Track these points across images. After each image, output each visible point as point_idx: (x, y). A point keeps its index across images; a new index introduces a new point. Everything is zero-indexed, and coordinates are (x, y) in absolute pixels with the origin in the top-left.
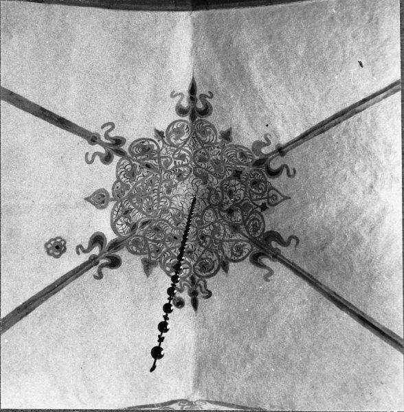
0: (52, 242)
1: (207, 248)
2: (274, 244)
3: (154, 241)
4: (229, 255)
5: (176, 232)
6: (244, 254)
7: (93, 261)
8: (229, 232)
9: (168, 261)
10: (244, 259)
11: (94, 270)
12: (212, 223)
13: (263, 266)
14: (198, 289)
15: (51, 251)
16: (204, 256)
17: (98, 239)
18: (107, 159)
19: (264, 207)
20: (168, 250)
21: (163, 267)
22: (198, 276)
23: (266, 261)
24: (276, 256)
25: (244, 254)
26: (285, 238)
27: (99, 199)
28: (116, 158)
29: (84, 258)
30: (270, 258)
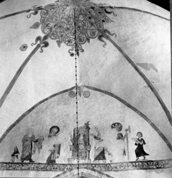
0: (22, 47)
1: (81, 32)
2: (107, 34)
3: (60, 32)
4: (90, 36)
5: (68, 26)
6: (96, 36)
7: (39, 46)
8: (89, 25)
9: (66, 40)
10: (95, 37)
11: (39, 49)
12: (82, 21)
13: (103, 41)
14: (79, 49)
15: (22, 50)
16: (80, 35)
17: (38, 38)
18: (36, 13)
19: (103, 21)
20: (66, 35)
21: (65, 43)
22: (78, 43)
23: (104, 39)
24: (108, 38)
25: (96, 36)
26: (112, 33)
27: (36, 26)
28: (39, 11)
29: (35, 46)
30: (105, 38)
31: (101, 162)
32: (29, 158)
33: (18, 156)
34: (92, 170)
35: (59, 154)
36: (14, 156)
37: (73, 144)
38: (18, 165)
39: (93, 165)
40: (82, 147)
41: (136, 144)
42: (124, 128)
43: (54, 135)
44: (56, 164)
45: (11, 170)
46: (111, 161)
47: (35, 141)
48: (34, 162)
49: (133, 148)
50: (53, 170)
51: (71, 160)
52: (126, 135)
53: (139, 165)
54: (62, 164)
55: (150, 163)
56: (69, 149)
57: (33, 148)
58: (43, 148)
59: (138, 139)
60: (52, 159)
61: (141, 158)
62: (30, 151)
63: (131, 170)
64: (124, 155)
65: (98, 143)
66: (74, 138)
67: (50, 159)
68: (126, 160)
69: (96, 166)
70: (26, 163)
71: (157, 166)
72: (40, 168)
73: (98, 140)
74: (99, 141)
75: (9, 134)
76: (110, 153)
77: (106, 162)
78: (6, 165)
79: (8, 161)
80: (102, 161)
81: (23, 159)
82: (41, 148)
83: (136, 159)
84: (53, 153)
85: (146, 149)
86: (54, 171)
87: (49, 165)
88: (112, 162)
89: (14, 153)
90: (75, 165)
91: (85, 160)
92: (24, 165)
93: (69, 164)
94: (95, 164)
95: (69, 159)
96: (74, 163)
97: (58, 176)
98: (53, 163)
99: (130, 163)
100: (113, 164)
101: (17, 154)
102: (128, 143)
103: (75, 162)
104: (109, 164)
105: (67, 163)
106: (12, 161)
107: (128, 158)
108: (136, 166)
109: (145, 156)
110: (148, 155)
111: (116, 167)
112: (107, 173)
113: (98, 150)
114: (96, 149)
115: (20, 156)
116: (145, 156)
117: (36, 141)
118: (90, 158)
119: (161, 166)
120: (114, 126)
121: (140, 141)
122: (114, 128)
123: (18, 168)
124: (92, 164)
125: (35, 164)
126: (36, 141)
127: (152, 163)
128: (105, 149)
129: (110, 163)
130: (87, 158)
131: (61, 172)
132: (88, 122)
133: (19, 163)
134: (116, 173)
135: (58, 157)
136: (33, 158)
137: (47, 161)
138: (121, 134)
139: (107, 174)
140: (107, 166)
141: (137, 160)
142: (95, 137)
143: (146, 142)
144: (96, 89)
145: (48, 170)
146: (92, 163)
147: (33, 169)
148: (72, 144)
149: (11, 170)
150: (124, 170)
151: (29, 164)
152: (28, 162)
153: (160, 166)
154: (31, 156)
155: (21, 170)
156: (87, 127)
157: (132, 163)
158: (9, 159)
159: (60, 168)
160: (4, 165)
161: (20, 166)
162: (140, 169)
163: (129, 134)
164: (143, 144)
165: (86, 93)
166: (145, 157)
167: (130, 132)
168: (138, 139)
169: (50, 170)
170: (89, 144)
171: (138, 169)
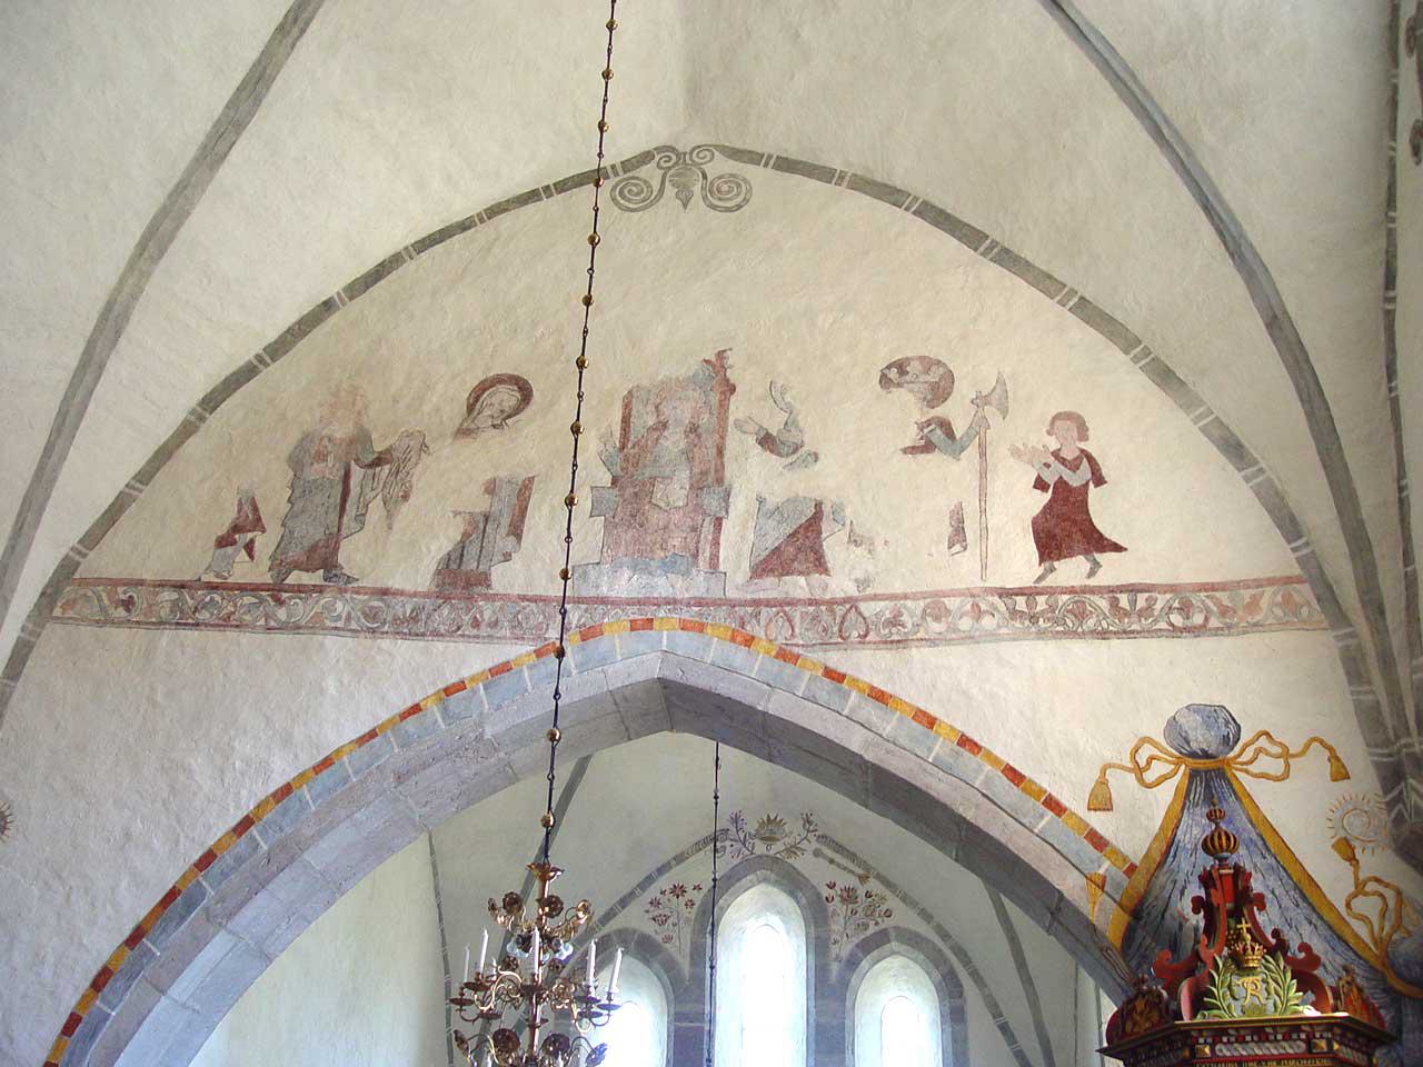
31: (798, 585)
32: (324, 558)
33: (256, 544)
34: (733, 639)
35: (519, 537)
36: (230, 550)
37: (615, 481)
38: (248, 600)
39: (740, 611)
40: (676, 491)
41: (1040, 485)
42: (963, 391)
43: (494, 426)
46: (862, 583)
47: (371, 458)
48: (349, 579)
50: (475, 632)
51: (593, 574)
52: (979, 427)
53: (1052, 608)
54: (535, 599)
55: (1133, 602)
58: (412, 499)
59: (1056, 454)
60: (470, 564)
61: (1071, 571)
62: (334, 516)
63: (993, 637)
64: (957, 547)
65: (781, 474)
66: (623, 447)
69: (757, 615)
70: (299, 589)
71: (1177, 619)
72: (389, 619)
73: (780, 455)
74: (790, 460)
75: (214, 420)
76: (858, 530)
77: (826, 587)
78: (175, 596)
80: (802, 580)
81: (281, 565)
82: (406, 497)
83: (1040, 571)
85: (1104, 511)
86: (477, 637)
87: (447, 599)
88: (869, 591)
89: (236, 528)
90: (615, 603)
92: (285, 595)
94: (756, 603)
96: (613, 594)
97: (503, 668)
98: (478, 589)
100: (875, 598)
101: (250, 535)
102: (983, 475)
103: (624, 584)
104: (851, 602)
106: (218, 576)
107: (984, 567)
108: (1034, 619)
109: (1105, 558)
110: (1117, 548)
111: (894, 622)
112: (835, 659)
113: (777, 516)
114: (770, 506)
115: (265, 543)
116: (1098, 556)
117: (379, 461)
118: (722, 568)
119: (1206, 619)
120: (895, 374)
121: (1074, 466)
122: (899, 385)
123: (247, 618)
124: (733, 604)
126: (379, 461)
128: (826, 509)
129: (852, 591)
130: (703, 562)
132: (721, 355)
134: (886, 657)
135: (507, 557)
136: (352, 554)
137: (438, 572)
138: (946, 426)
139: (831, 665)
140: (832, 612)
141: (1040, 578)
142: (767, 441)
144: (786, 165)
145: (437, 634)
146: (732, 594)
147: (340, 624)
148: (606, 479)
149: (206, 625)
150: (949, 642)
151: (320, 590)
152: (316, 578)
153: (1198, 619)
154: (336, 550)
156: (718, 378)
157: (1005, 593)
159: (518, 625)
160: (168, 595)
161: (262, 601)
162: (1057, 635)
165: (725, 188)
166: (1097, 564)
167: (1004, 412)
168: (1056, 454)
169: (455, 631)
170: (720, 481)
171: (1041, 634)
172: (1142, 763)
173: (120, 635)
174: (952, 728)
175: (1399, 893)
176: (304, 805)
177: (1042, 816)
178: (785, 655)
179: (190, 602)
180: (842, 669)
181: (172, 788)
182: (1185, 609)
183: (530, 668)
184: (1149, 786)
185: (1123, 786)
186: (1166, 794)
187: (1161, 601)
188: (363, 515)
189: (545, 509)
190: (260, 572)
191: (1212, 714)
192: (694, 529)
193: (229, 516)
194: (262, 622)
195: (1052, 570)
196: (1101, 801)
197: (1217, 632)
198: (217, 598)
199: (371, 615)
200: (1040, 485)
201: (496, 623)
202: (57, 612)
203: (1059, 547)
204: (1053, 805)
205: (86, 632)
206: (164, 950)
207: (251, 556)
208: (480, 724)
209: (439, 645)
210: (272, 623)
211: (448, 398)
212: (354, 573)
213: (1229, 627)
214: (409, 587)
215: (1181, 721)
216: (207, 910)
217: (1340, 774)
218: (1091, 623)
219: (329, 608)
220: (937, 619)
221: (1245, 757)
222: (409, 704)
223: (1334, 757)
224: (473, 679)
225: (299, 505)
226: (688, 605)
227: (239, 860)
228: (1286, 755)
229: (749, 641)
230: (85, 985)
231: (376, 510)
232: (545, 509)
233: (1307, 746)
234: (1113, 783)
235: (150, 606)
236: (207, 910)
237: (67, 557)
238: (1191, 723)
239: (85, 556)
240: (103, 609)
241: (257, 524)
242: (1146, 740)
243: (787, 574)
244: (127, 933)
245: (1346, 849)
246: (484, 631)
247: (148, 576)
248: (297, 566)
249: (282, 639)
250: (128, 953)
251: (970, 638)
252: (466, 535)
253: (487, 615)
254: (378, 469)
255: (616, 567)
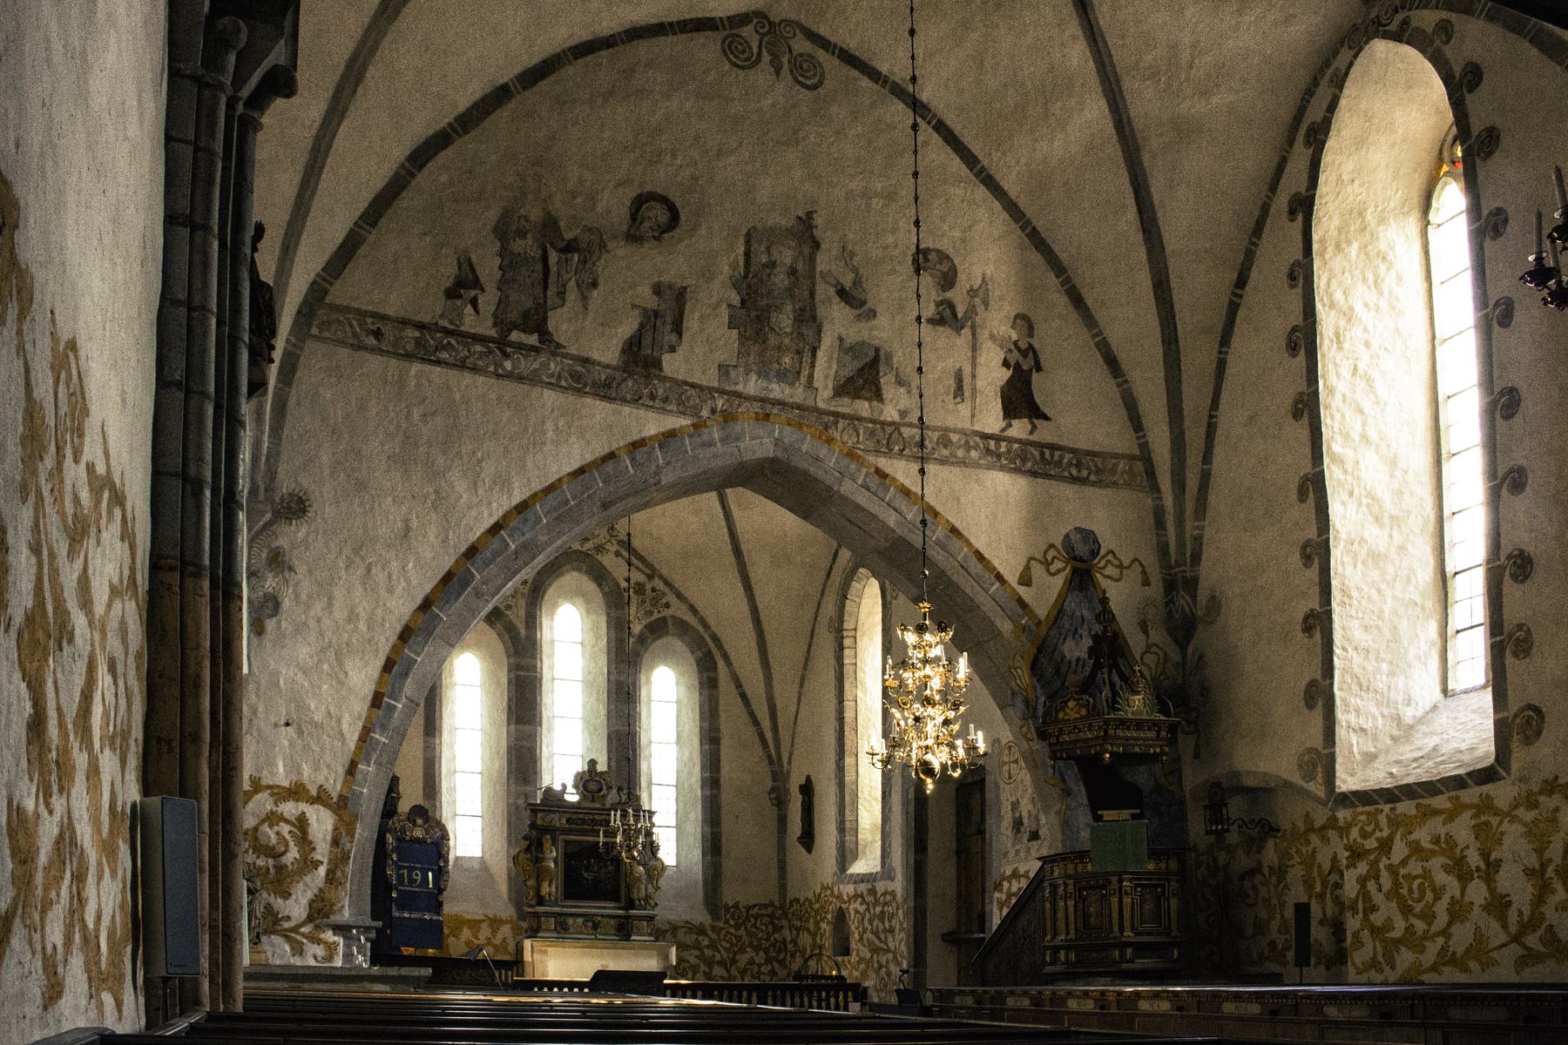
31: (863, 408)
32: (536, 322)
35: (680, 334)
36: (459, 302)
38: (479, 348)
39: (826, 419)
40: (784, 320)
41: (1006, 364)
44: (665, 379)
45: (447, 364)
48: (559, 346)
49: (992, 374)
51: (733, 373)
53: (1009, 451)
54: (693, 386)
55: (1052, 455)
56: (726, 319)
57: (552, 279)
58: (601, 287)
61: (1019, 429)
62: (538, 291)
63: (977, 465)
64: (958, 399)
67: (635, 349)
68: (967, 426)
70: (520, 347)
71: (1074, 472)
72: (589, 382)
75: (423, 178)
78: (417, 334)
79: (427, 319)
80: (866, 404)
84: (650, 319)
87: (631, 374)
88: (907, 420)
90: (747, 398)
91: (792, 384)
92: (509, 350)
93: (722, 392)
94: (836, 414)
95: (724, 370)
96: (746, 391)
97: (671, 435)
98: (653, 371)
99: (978, 439)
101: (473, 293)
102: (974, 349)
105: (716, 384)
106: (451, 322)
108: (999, 456)
109: (1039, 423)
110: (1047, 418)
112: (883, 463)
114: (846, 345)
115: (488, 300)
117: (570, 247)
118: (816, 384)
123: (480, 363)
125: (565, 356)
126: (570, 247)
127: (1057, 453)
129: (896, 418)
130: (803, 379)
131: (684, 422)
133: (482, 339)
135: (673, 349)
136: (561, 323)
137: (623, 351)
139: (880, 465)
141: (1003, 430)
143: (1043, 364)
145: (624, 401)
146: (821, 405)
147: (553, 380)
149: (447, 364)
152: (533, 339)
153: (1085, 473)
154: (545, 319)
155: (498, 376)
157: (986, 437)
158: (432, 308)
161: (490, 352)
163: (980, 309)
164: (1031, 370)
169: (636, 401)
172: (1049, 559)
173: (375, 363)
174: (948, 521)
175: (1166, 654)
176: (538, 520)
177: (993, 584)
178: (851, 455)
179: (432, 342)
180: (888, 470)
181: (437, 492)
182: (1079, 465)
183: (691, 436)
184: (1052, 574)
185: (1038, 571)
186: (1058, 582)
187: (1068, 457)
188: (564, 293)
189: (697, 315)
190: (487, 328)
191: (1088, 536)
192: (798, 352)
193: (448, 272)
194: (492, 369)
195: (1010, 425)
196: (1025, 580)
197: (1094, 484)
198: (453, 342)
199: (576, 377)
200: (1006, 364)
201: (667, 398)
202: (314, 331)
203: (1014, 410)
204: (999, 577)
205: (344, 352)
206: (448, 616)
207: (477, 311)
208: (657, 474)
209: (627, 410)
210: (500, 371)
211: (613, 206)
212: (562, 340)
213: (1101, 481)
214: (603, 359)
215: (1072, 537)
216: (474, 588)
217: (1146, 583)
218: (1029, 465)
219: (545, 366)
220: (946, 447)
221: (1102, 563)
222: (607, 451)
223: (1144, 572)
224: (651, 438)
225: (510, 275)
226: (792, 407)
227: (496, 554)
228: (1121, 566)
229: (830, 441)
230: (393, 639)
231: (572, 296)
232: (697, 315)
233: (1132, 562)
234: (1033, 571)
235: (397, 339)
236: (474, 588)
237: (314, 282)
238: (1075, 538)
239: (331, 284)
240: (355, 335)
241: (476, 284)
242: (1052, 546)
243: (859, 398)
244: (419, 601)
245: (1144, 627)
246: (658, 403)
247: (391, 311)
248: (515, 326)
249: (509, 387)
250: (422, 617)
251: (963, 463)
252: (642, 325)
253: (660, 391)
254: (569, 255)
255: (748, 372)
